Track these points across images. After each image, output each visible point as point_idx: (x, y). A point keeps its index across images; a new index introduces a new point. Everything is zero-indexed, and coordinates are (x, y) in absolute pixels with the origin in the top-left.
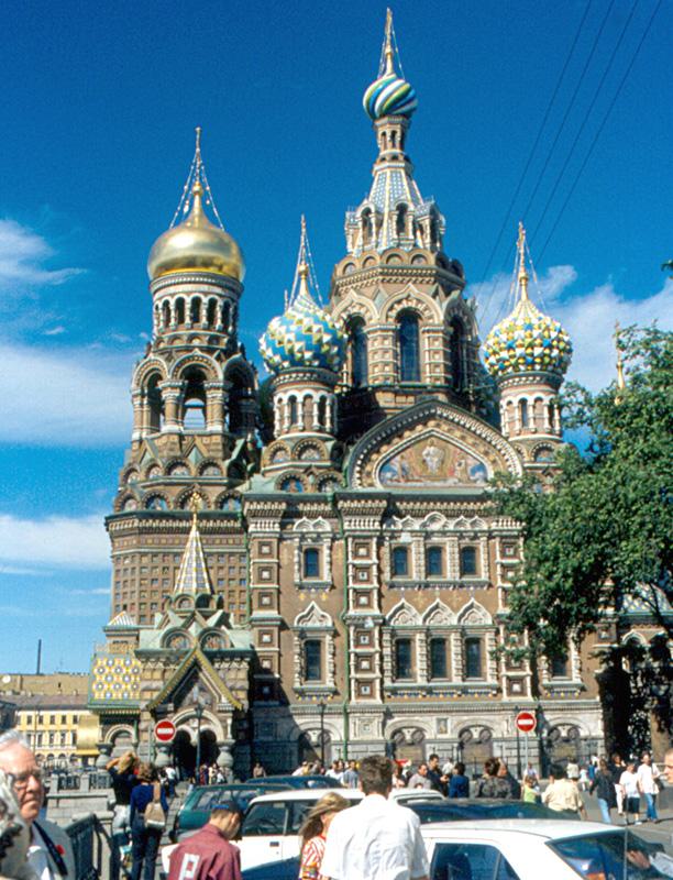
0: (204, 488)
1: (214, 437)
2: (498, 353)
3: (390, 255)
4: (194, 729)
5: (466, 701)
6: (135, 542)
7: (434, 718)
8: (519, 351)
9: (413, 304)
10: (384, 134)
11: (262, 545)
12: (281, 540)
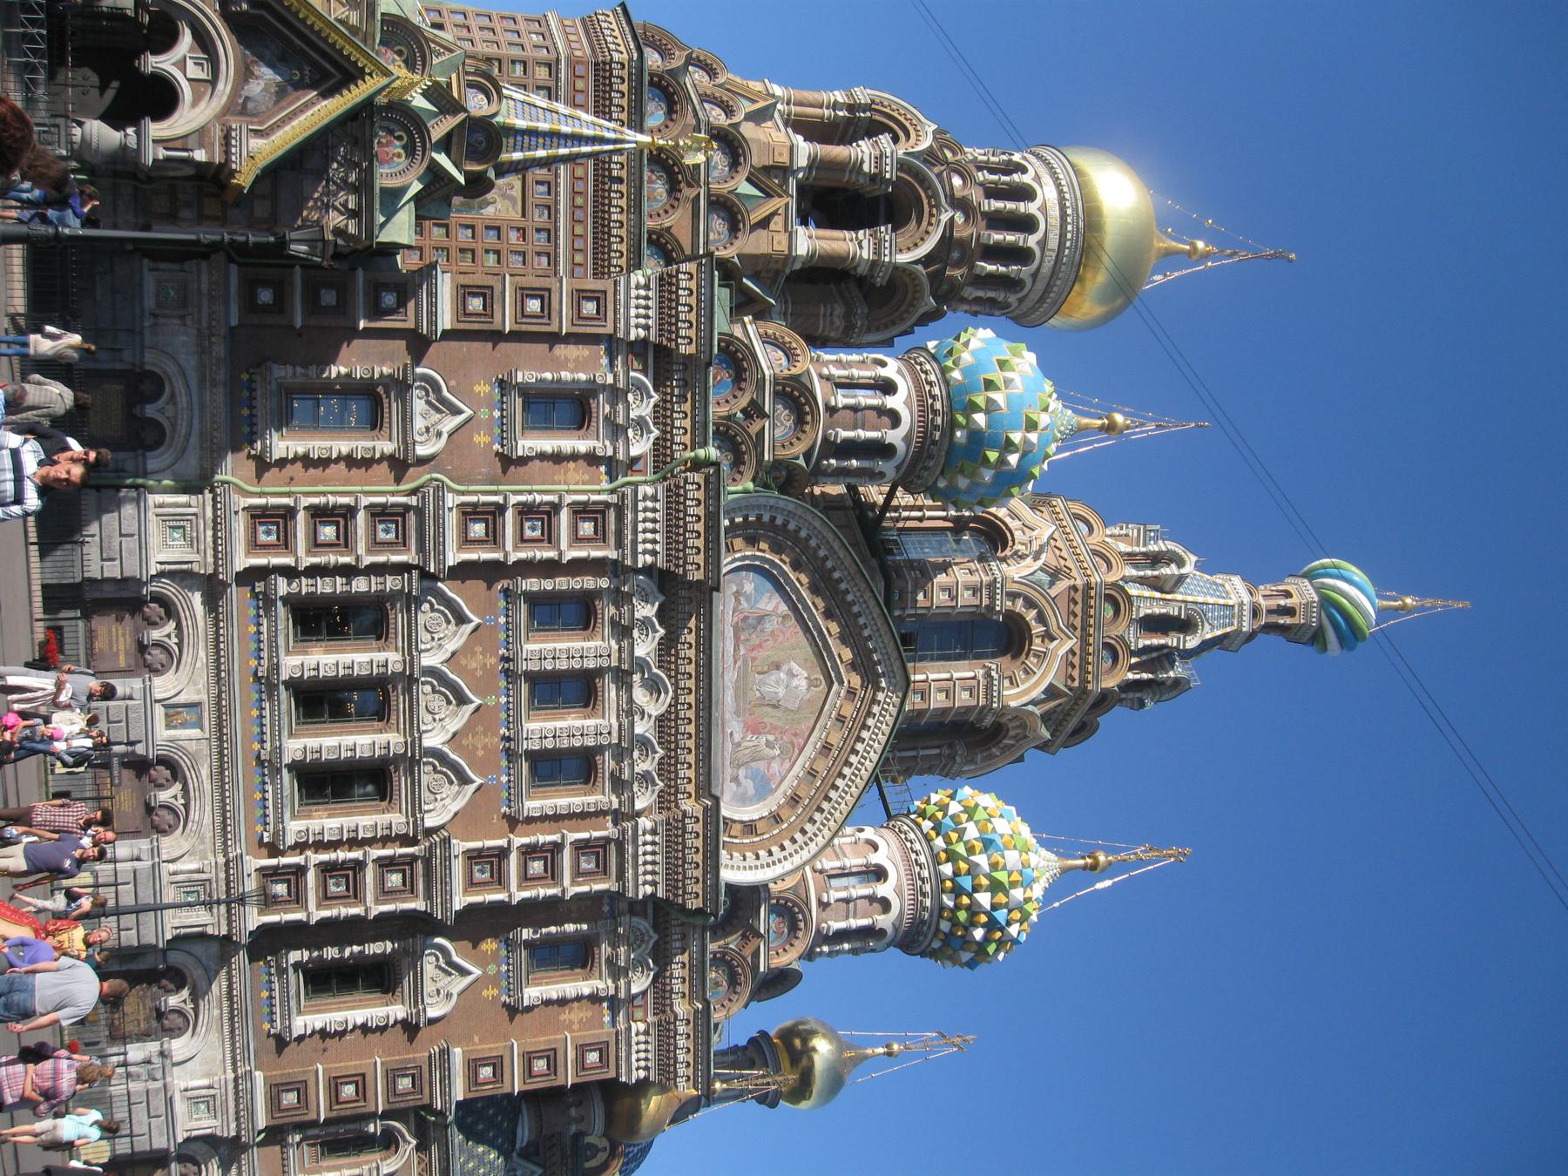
0: (689, 205)
1: (784, 237)
2: (970, 819)
3: (1116, 599)
4: (182, 65)
5: (242, 768)
6: (578, 53)
7: (204, 697)
8: (981, 860)
9: (1037, 645)
10: (1288, 595)
11: (598, 297)
12: (613, 345)
